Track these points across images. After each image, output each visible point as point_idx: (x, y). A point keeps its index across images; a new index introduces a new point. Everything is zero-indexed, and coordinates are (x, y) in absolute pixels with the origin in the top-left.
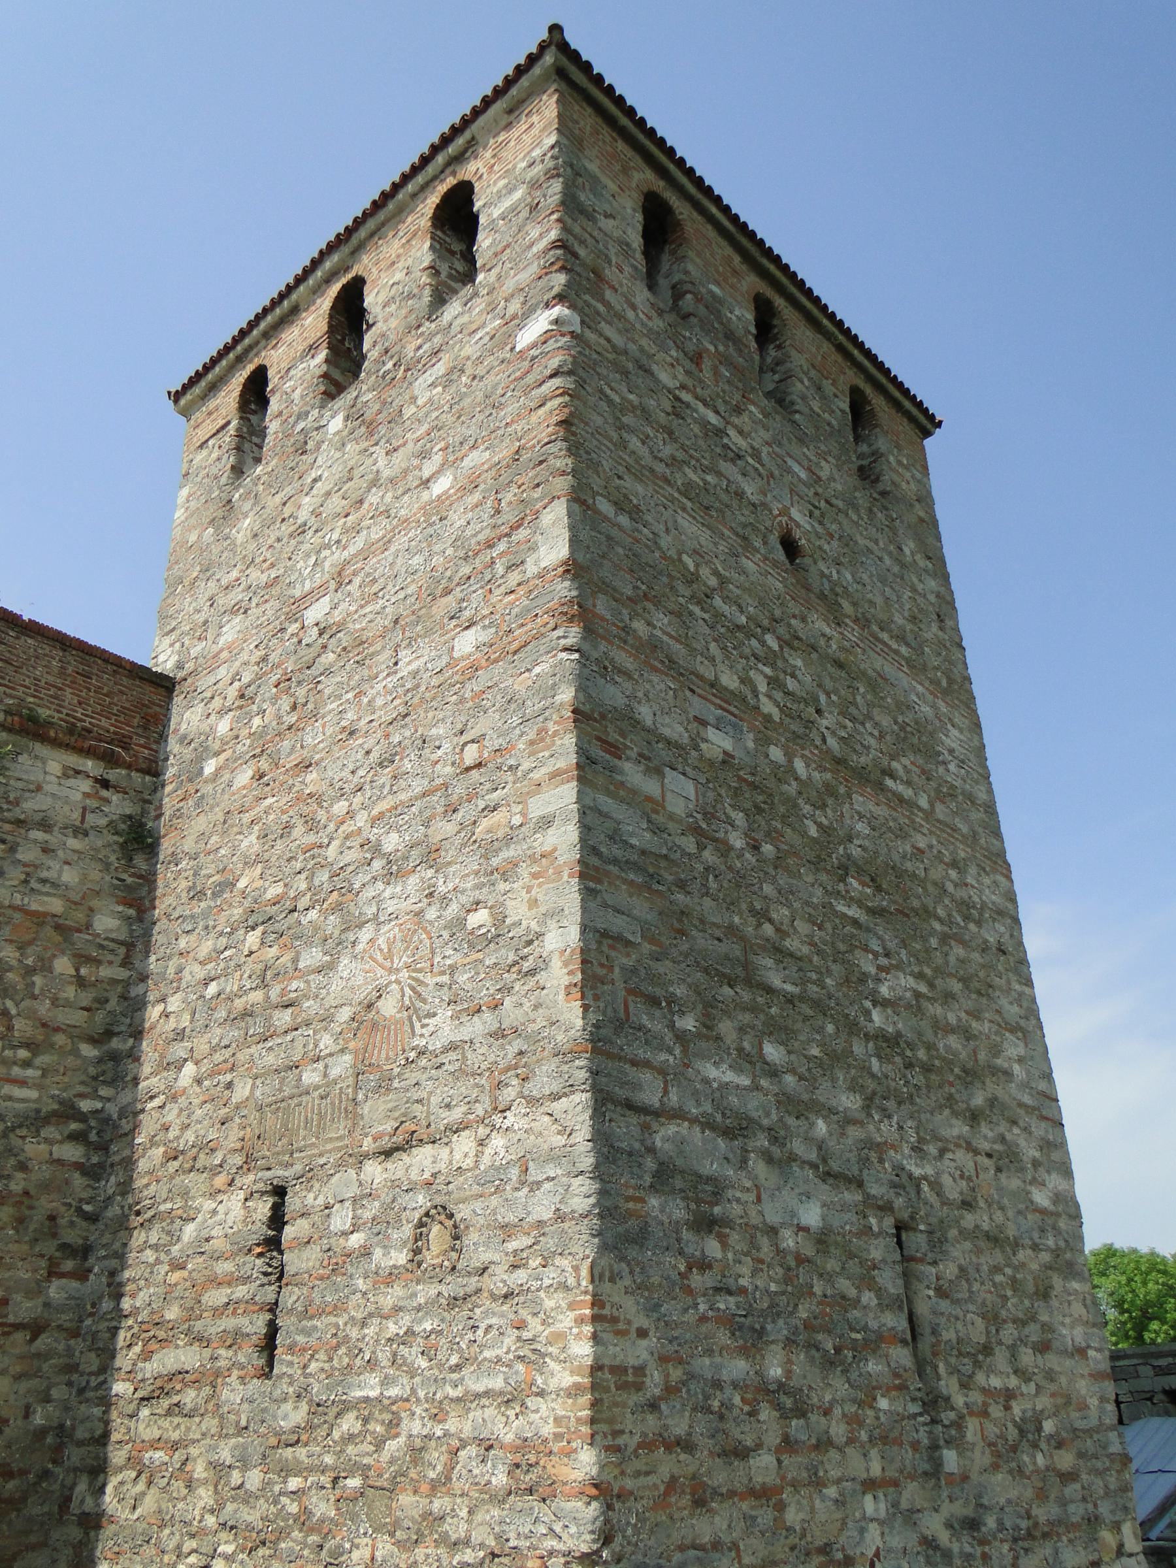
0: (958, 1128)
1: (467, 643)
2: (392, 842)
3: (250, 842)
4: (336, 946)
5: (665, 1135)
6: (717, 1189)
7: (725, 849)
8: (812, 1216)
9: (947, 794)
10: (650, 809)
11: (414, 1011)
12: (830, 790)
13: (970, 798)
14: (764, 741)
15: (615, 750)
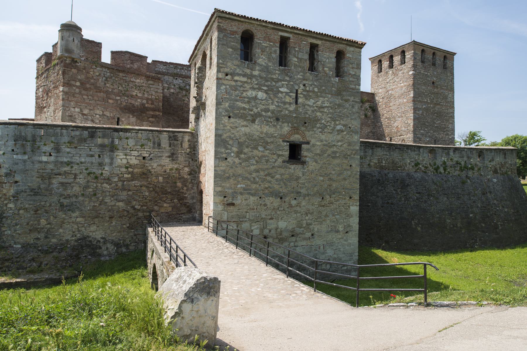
0: (442, 133)
1: (405, 100)
2: (399, 115)
3: (385, 112)
4: (395, 122)
5: (418, 135)
6: (421, 138)
7: (424, 115)
8: (428, 140)
9: (447, 102)
10: (418, 114)
11: (401, 127)
12: (434, 107)
13: (451, 102)
14: (428, 105)
15: (416, 110)
